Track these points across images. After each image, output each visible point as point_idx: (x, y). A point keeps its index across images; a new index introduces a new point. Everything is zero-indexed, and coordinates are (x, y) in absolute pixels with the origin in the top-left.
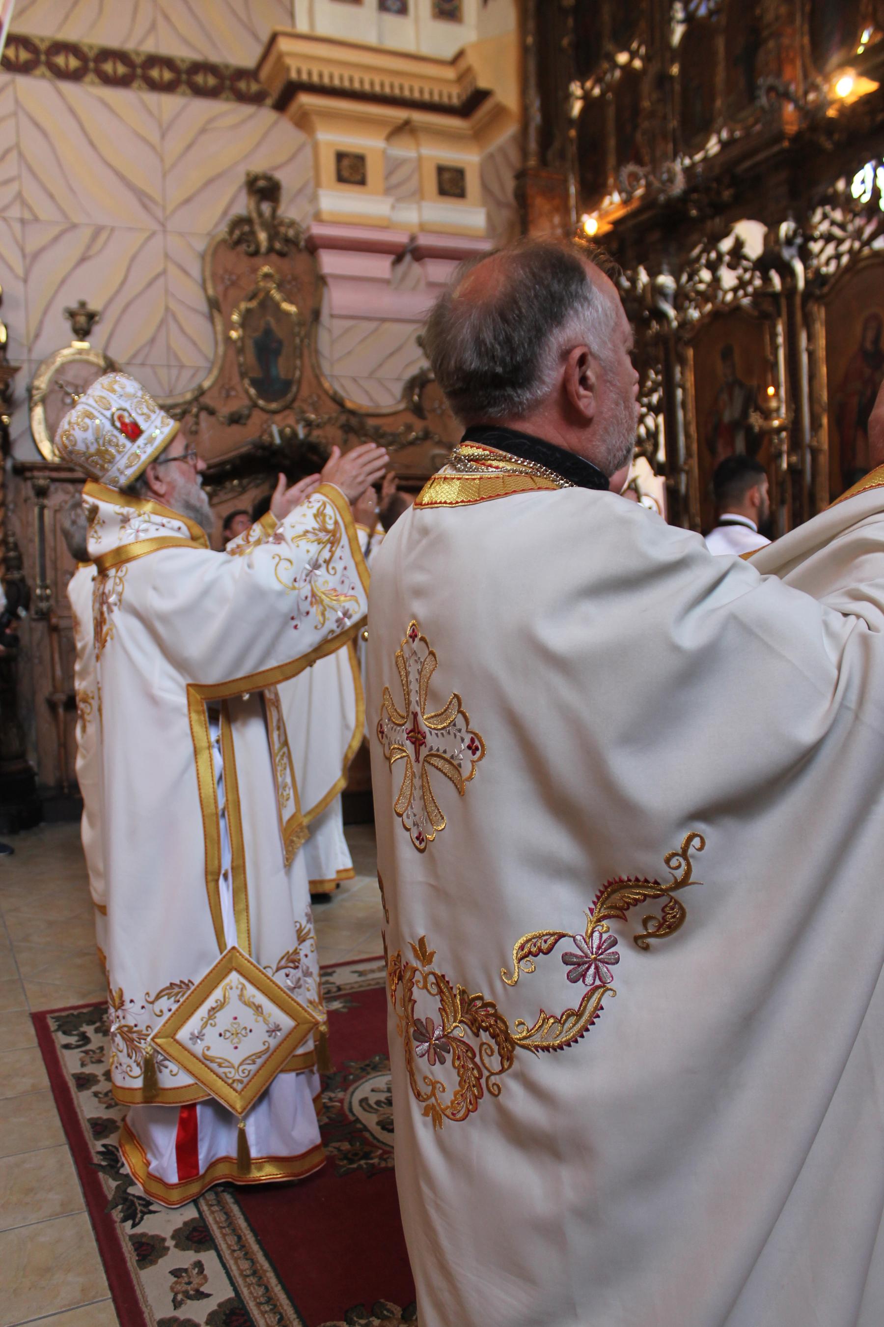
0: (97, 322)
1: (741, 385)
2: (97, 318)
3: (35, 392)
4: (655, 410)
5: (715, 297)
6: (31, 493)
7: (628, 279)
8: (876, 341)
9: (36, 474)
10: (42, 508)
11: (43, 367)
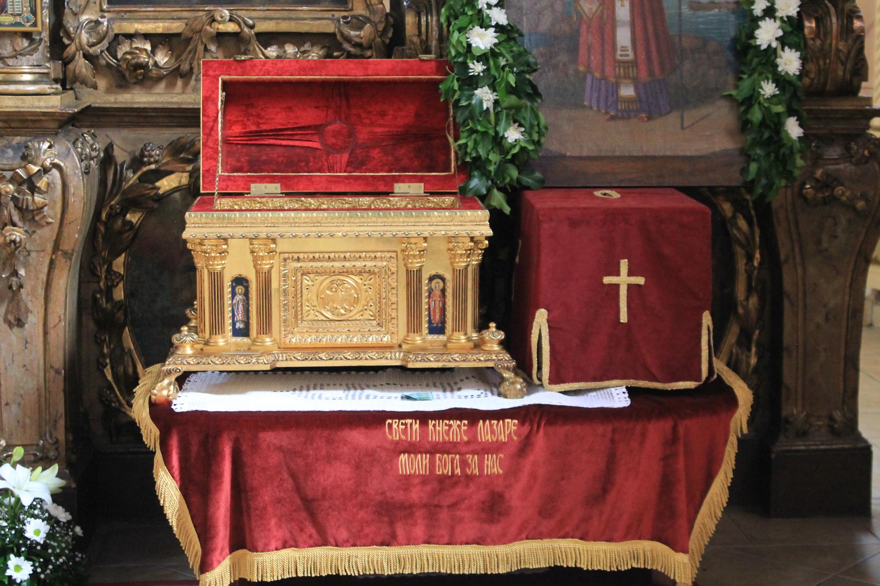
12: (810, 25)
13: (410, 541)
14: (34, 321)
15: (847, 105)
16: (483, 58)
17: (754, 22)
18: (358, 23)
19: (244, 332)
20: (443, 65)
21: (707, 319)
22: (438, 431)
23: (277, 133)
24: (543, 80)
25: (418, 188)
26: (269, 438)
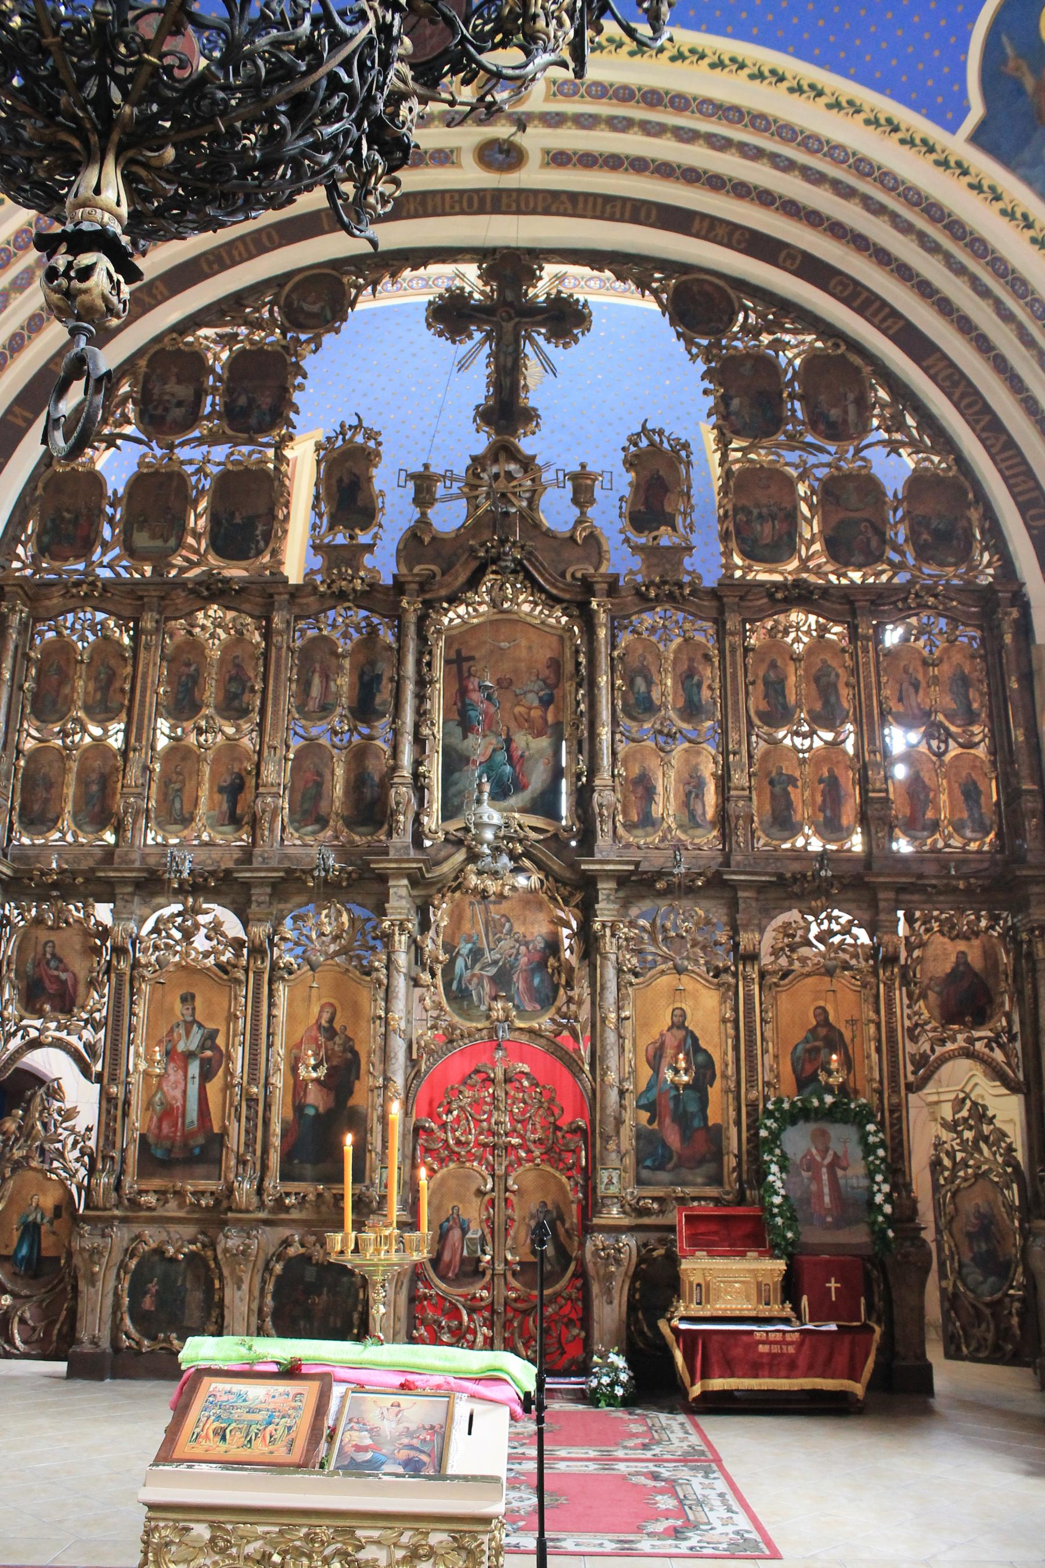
1: (200, 1026)
4: (96, 1027)
5: (188, 954)
7: (77, 909)
8: (331, 1020)
12: (895, 1195)
13: (763, 1377)
14: (616, 1302)
15: (912, 1225)
16: (778, 1206)
17: (873, 1194)
18: (727, 1193)
19: (699, 1303)
20: (763, 1209)
21: (863, 1300)
22: (772, 1336)
23: (703, 1234)
24: (799, 1215)
25: (755, 1254)
26: (715, 1337)
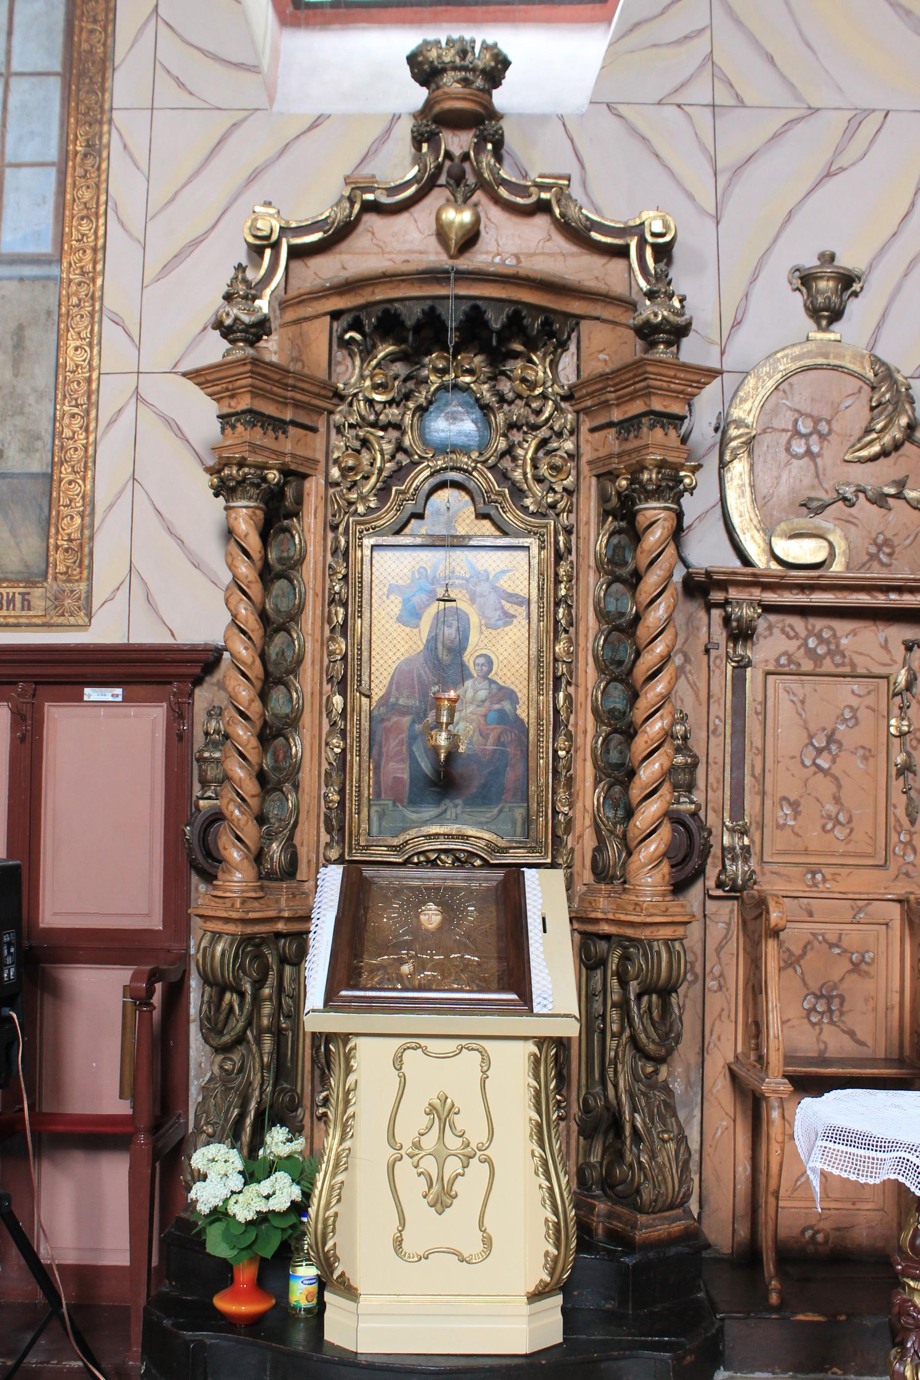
0: (855, 294)
2: (856, 287)
3: (733, 432)
6: (719, 635)
9: (733, 593)
10: (742, 665)
11: (751, 381)
